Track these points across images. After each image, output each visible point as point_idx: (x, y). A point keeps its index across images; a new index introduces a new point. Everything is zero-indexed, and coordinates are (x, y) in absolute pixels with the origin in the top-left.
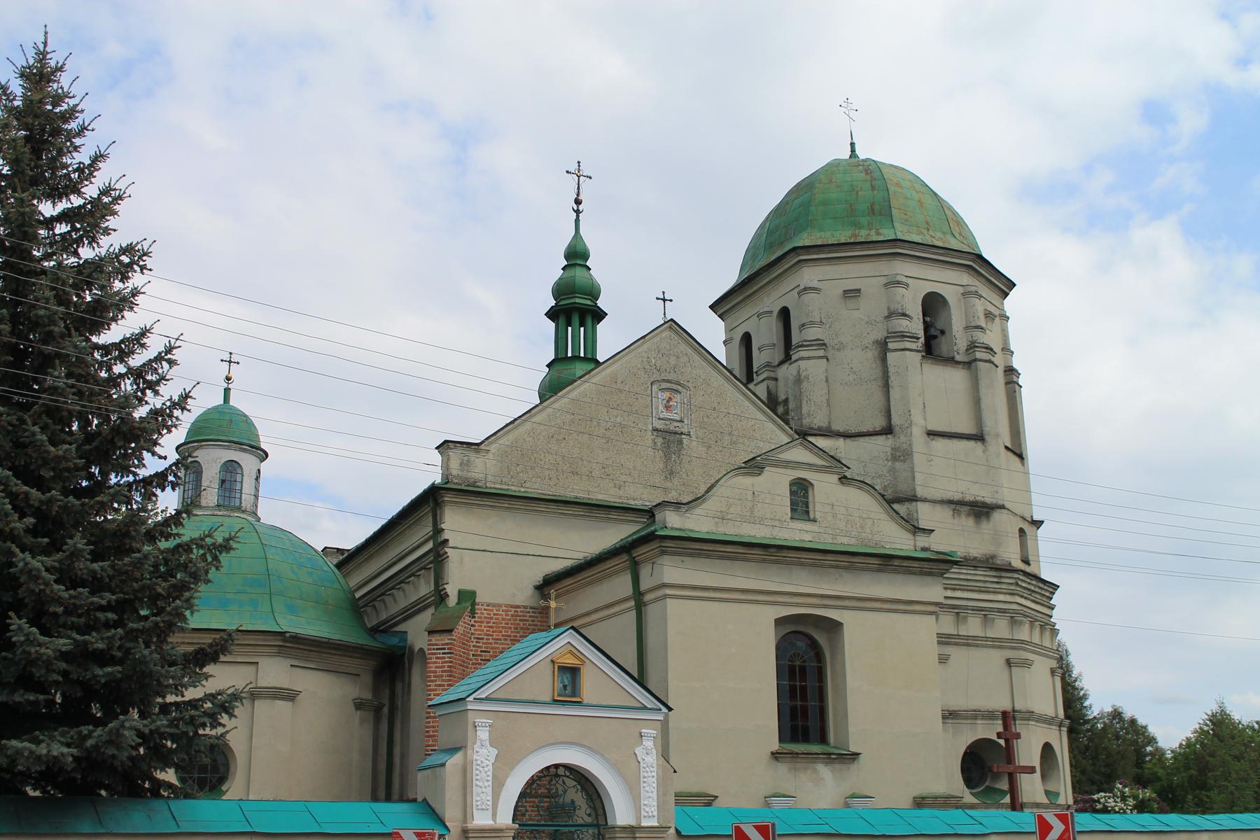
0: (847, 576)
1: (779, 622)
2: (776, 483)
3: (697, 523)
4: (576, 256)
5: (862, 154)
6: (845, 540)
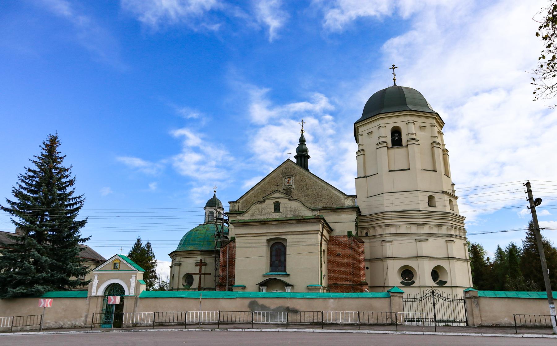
0: (287, 226)
1: (268, 241)
2: (269, 204)
3: (246, 217)
4: (302, 141)
5: (398, 85)
6: (289, 216)
